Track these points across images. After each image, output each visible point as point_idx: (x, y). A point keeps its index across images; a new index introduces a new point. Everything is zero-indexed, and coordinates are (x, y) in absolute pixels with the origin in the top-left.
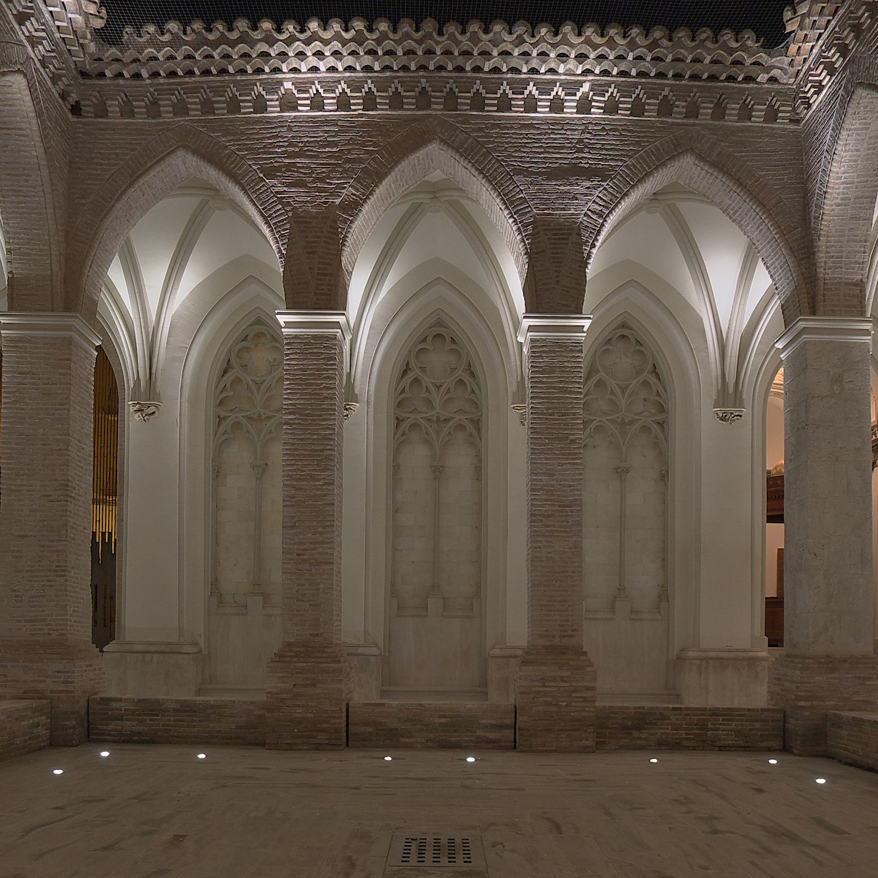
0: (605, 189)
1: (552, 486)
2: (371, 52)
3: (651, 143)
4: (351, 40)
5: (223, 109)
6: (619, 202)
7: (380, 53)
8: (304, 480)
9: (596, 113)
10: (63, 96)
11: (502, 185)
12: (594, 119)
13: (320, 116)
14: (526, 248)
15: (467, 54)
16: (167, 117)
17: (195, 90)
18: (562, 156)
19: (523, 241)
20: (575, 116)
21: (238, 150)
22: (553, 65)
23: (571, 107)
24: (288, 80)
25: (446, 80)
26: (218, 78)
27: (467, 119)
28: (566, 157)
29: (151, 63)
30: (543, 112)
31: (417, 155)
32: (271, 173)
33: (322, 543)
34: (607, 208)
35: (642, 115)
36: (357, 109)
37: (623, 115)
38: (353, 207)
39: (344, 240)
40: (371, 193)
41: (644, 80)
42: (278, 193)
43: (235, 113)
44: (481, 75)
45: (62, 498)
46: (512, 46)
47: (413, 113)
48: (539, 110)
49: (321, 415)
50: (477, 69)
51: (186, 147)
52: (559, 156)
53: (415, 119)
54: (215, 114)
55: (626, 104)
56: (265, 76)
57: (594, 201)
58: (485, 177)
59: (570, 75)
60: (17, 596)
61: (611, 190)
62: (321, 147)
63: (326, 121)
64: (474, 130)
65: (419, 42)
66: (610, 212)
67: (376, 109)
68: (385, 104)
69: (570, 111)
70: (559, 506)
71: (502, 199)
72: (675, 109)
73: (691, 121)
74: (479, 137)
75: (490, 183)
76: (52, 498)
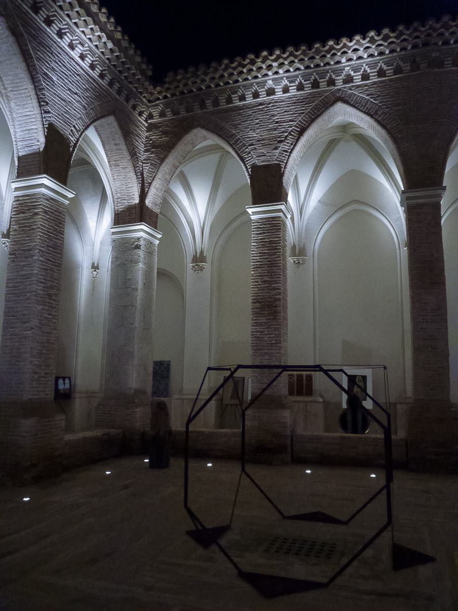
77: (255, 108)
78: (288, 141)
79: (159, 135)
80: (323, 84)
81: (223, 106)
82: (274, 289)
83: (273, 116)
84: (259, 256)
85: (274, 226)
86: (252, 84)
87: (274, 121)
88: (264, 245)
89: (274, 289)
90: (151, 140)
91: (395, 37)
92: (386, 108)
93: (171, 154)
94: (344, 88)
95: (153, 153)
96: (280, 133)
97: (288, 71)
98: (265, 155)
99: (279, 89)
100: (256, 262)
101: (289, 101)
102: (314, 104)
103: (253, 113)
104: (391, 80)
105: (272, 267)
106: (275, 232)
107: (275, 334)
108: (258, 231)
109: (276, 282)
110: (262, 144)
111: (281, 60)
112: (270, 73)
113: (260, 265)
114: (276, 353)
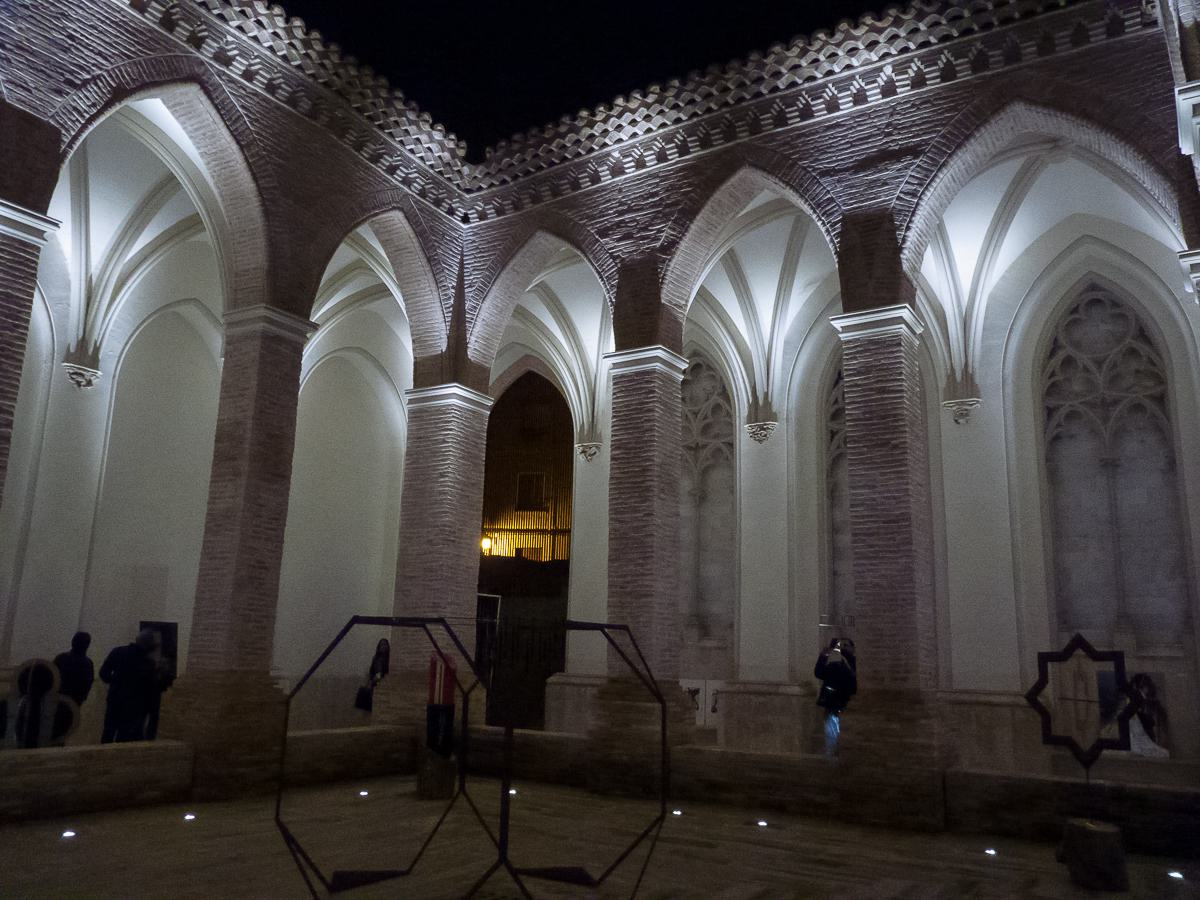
0: (919, 166)
1: (874, 500)
2: (676, 107)
3: (968, 103)
4: (654, 103)
6: (935, 175)
7: (682, 104)
9: (903, 92)
12: (904, 98)
13: (644, 173)
14: (836, 248)
15: (759, 80)
16: (529, 207)
17: (545, 180)
18: (870, 145)
19: (832, 241)
20: (882, 101)
21: (581, 220)
22: (847, 62)
23: (875, 95)
24: (614, 150)
25: (748, 108)
26: (563, 165)
27: (772, 137)
28: (879, 143)
29: (510, 169)
30: (847, 107)
31: (729, 184)
32: (603, 233)
33: (643, 575)
34: (921, 185)
35: (955, 78)
36: (674, 157)
37: (932, 85)
38: (670, 247)
39: (663, 278)
40: (686, 231)
41: (948, 43)
42: (610, 249)
44: (779, 93)
46: (797, 60)
48: (841, 107)
50: (776, 89)
51: (541, 228)
52: (866, 146)
53: (726, 151)
54: (562, 195)
55: (932, 73)
56: (596, 153)
57: (907, 182)
58: (792, 187)
59: (867, 64)
61: (925, 166)
62: (645, 199)
64: (780, 146)
65: (711, 85)
66: (926, 188)
67: (689, 153)
68: (696, 146)
69: (875, 98)
70: (884, 522)
71: (810, 205)
72: (992, 60)
73: (1015, 66)
74: (785, 150)
75: (797, 191)
78: (88, 94)
80: (183, 31)
85: (20, 263)
87: (63, 28)
91: (318, 52)
96: (74, 65)
98: (30, 91)
101: (107, 12)
104: (278, 108)
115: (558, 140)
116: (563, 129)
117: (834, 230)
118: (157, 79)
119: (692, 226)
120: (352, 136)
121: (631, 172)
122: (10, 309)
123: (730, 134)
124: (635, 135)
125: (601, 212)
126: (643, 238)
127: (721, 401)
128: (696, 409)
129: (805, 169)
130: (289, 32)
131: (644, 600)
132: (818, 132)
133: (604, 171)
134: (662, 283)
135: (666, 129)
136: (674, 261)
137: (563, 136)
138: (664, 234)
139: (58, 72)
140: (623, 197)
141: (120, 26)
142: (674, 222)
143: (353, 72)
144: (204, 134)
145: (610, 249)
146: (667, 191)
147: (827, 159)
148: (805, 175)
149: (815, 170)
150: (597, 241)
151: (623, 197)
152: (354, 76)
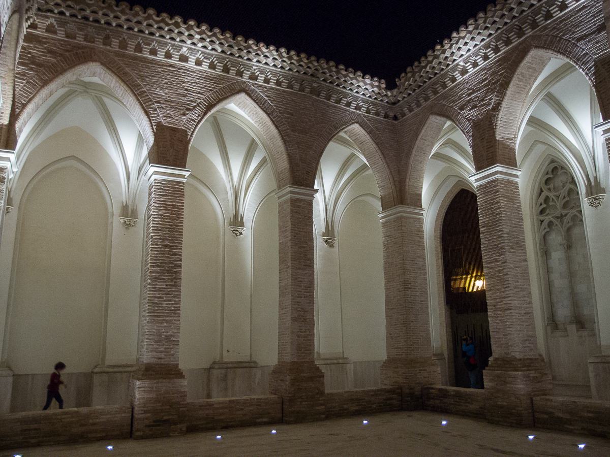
2: (486, 28)
5: (441, 89)
7: (489, 26)
8: (492, 263)
10: (386, 116)
11: (571, 53)
13: (478, 69)
14: (593, 83)
19: (590, 79)
26: (436, 77)
27: (545, 28)
31: (525, 62)
32: (462, 108)
33: (505, 297)
36: (492, 56)
39: (496, 126)
40: (505, 95)
42: (466, 116)
43: (446, 88)
45: (403, 289)
47: (519, 41)
49: (496, 224)
51: (432, 114)
53: (520, 44)
54: (439, 93)
58: (561, 53)
60: (392, 337)
63: (482, 70)
64: (551, 31)
68: (504, 45)
75: (564, 55)
76: (400, 290)
77: (165, 68)
78: (196, 112)
79: (42, 52)
80: (233, 72)
81: (130, 51)
82: (175, 254)
83: (184, 82)
84: (160, 218)
86: (167, 44)
87: (183, 87)
88: (166, 207)
89: (175, 254)
90: (30, 53)
91: (296, 60)
92: (280, 113)
93: (57, 79)
94: (249, 82)
95: (31, 69)
96: (189, 101)
97: (205, 47)
99: (192, 59)
100: (157, 224)
101: (200, 74)
102: (224, 85)
103: (162, 71)
104: (284, 91)
105: (174, 232)
106: (178, 197)
107: (175, 301)
108: (160, 192)
109: (177, 248)
110: (170, 105)
111: (204, 36)
112: (189, 42)
113: (161, 227)
114: (175, 320)
115: (429, 65)
116: (430, 59)
117: (590, 72)
118: (225, 96)
119: (508, 92)
120: (323, 94)
121: (472, 71)
122: (175, 211)
123: (520, 33)
124: (469, 50)
125: (459, 97)
126: (482, 105)
127: (572, 186)
128: (557, 194)
129: (567, 40)
130: (281, 56)
131: (508, 312)
132: (572, 16)
133: (457, 74)
134: (496, 128)
135: (485, 42)
136: (500, 114)
137: (431, 62)
138: (493, 100)
139: (182, 106)
140: (469, 86)
141: (206, 78)
142: (498, 92)
143: (316, 64)
144: (253, 113)
145: (466, 116)
146: (491, 76)
147: (579, 30)
148: (568, 44)
149: (573, 39)
150: (459, 113)
151: (469, 86)
152: (317, 66)
